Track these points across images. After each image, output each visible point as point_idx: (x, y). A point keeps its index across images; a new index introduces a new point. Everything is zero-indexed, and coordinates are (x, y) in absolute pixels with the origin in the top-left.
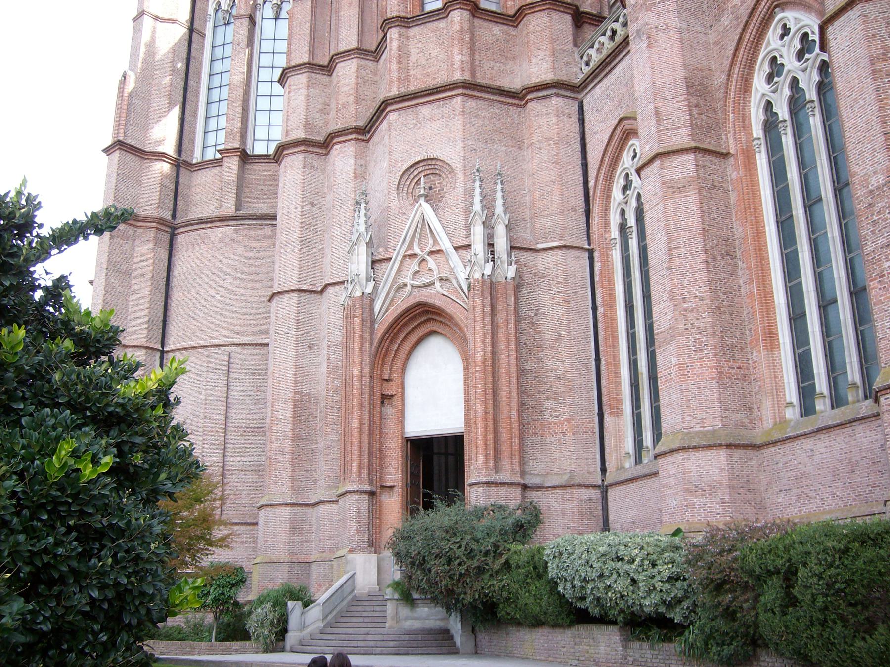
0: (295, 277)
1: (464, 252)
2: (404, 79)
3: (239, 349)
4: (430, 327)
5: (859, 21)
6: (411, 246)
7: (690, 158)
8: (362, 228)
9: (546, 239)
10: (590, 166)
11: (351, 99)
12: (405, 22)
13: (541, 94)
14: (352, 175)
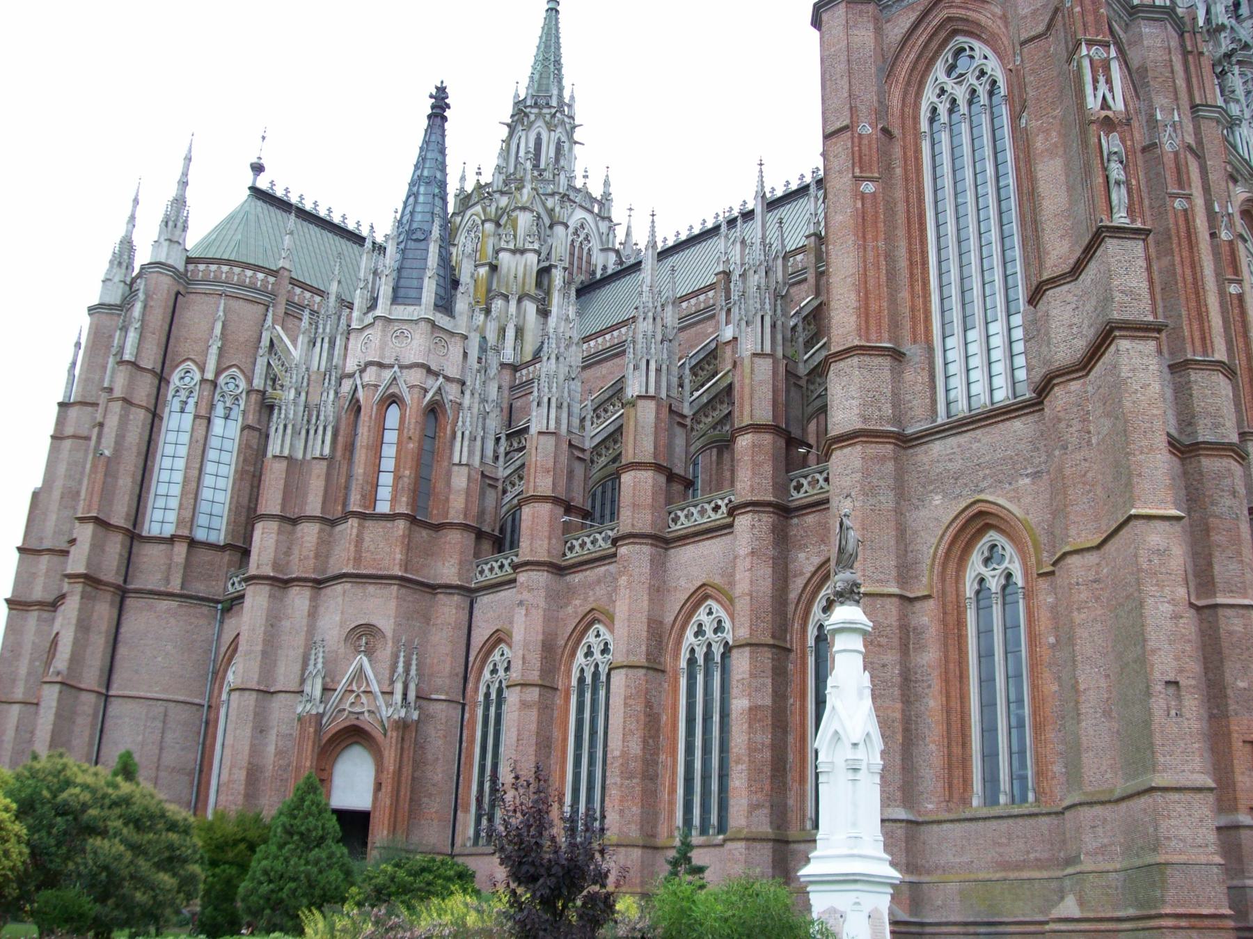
0: (256, 677)
1: (387, 696)
2: (358, 560)
3: (173, 704)
4: (354, 739)
5: (624, 677)
6: (351, 683)
7: (537, 690)
8: (320, 666)
9: (437, 692)
10: (471, 647)
11: (312, 554)
12: (362, 516)
13: (448, 591)
14: (306, 613)
